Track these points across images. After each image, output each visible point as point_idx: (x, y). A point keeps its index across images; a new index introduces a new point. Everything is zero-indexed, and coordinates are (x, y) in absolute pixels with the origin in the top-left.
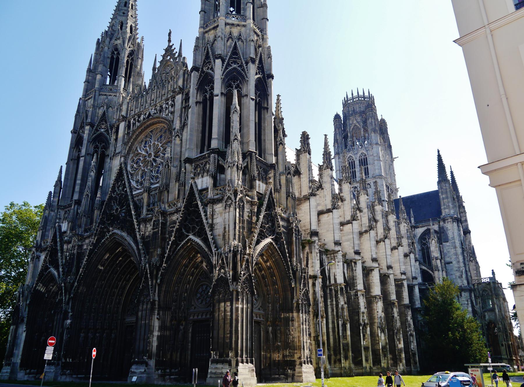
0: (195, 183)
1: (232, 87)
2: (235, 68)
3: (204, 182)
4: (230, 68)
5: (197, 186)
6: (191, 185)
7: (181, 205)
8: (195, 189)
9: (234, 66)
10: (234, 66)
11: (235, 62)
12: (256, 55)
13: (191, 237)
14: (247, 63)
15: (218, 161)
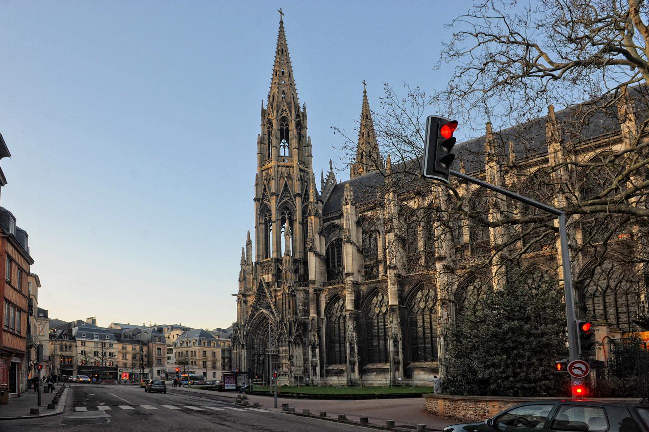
0: (263, 279)
1: (285, 214)
2: (286, 201)
3: (268, 278)
4: (283, 201)
5: (264, 281)
6: (261, 281)
7: (254, 290)
8: (263, 283)
9: (286, 199)
10: (286, 199)
11: (286, 196)
12: (302, 190)
13: (262, 310)
14: (295, 196)
15: (278, 266)
